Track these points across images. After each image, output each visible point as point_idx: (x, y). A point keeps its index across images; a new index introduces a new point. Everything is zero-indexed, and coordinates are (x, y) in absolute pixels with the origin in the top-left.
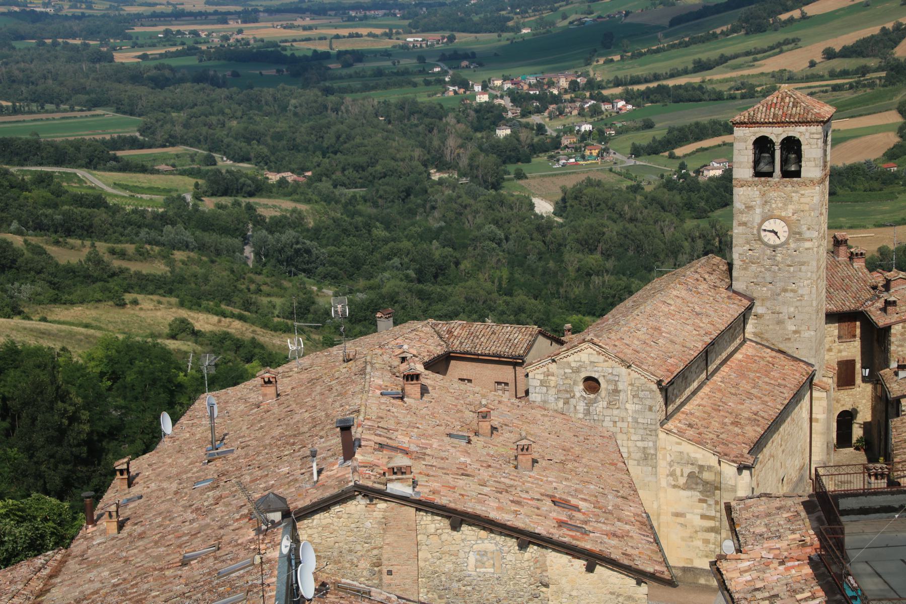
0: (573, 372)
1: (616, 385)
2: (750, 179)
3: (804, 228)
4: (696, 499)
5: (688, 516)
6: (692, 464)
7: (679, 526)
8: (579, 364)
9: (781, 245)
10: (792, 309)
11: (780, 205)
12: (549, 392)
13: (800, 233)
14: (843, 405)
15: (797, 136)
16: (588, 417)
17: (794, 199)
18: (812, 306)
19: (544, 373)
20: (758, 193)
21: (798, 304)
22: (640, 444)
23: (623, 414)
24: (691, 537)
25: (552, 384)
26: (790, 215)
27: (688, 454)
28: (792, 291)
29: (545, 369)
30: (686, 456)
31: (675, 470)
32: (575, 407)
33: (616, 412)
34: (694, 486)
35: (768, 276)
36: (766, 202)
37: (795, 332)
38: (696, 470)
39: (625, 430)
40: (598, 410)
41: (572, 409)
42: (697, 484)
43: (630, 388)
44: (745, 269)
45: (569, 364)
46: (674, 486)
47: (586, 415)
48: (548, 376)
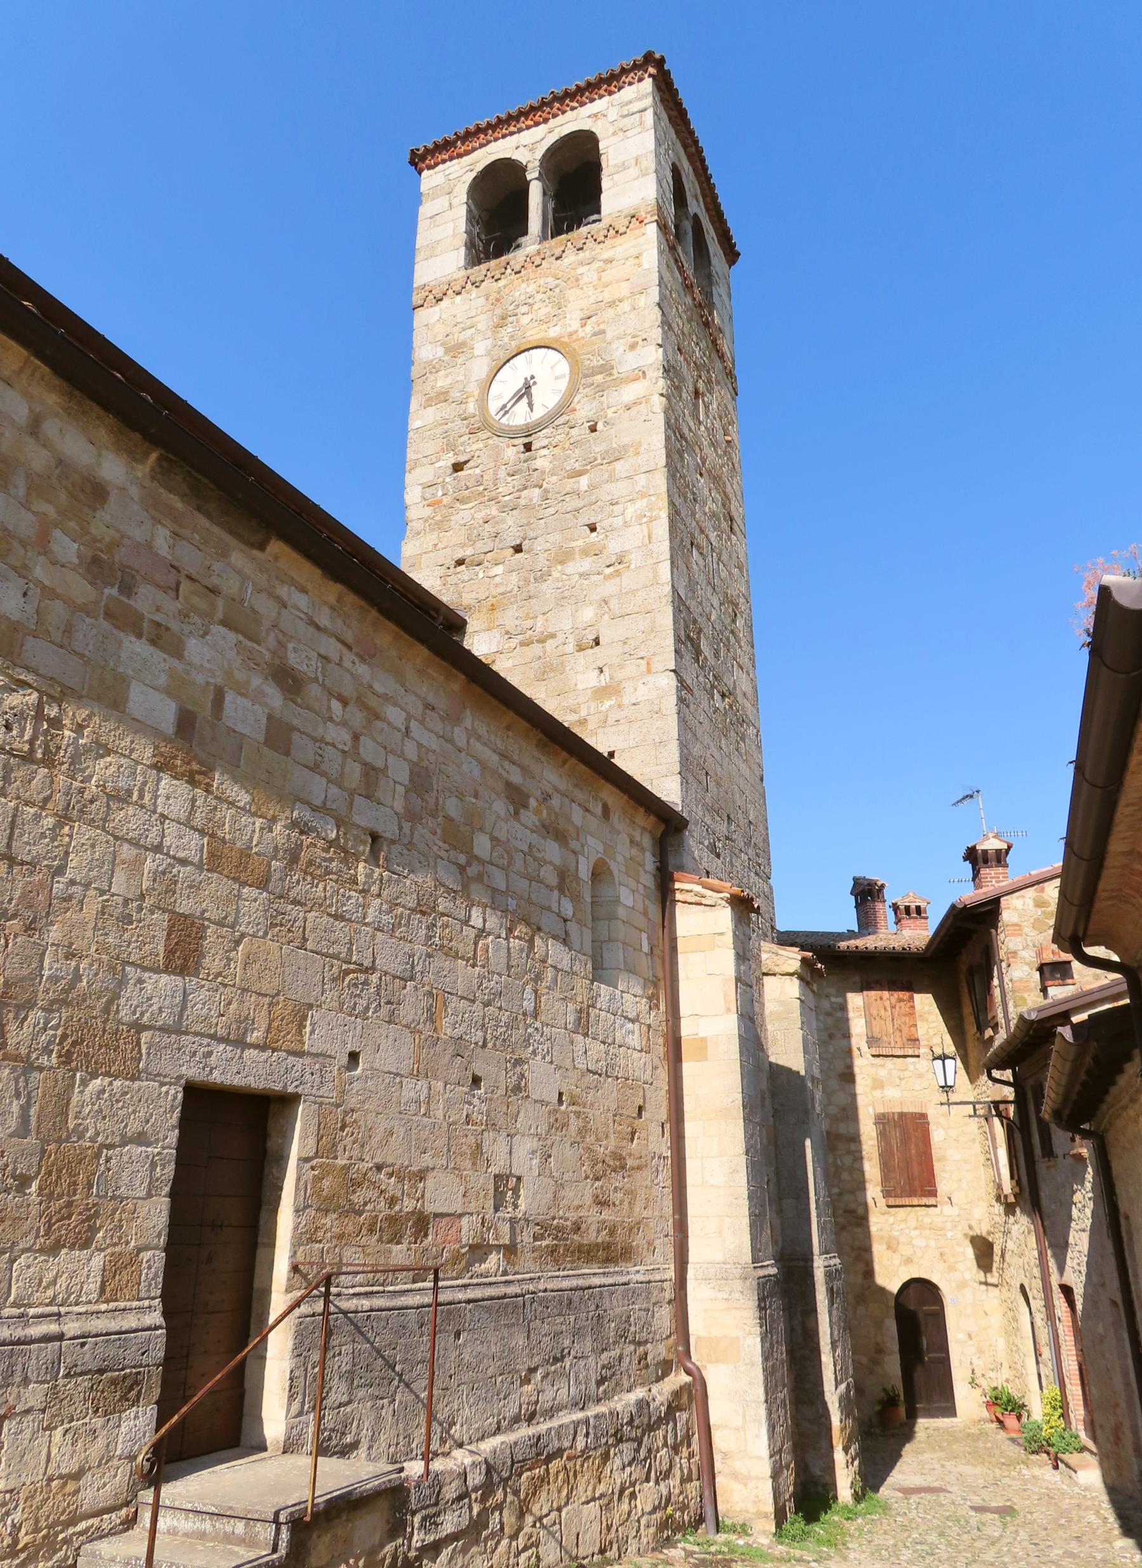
2: (463, 273)
3: (619, 348)
9: (550, 419)
10: (588, 614)
11: (543, 310)
13: (606, 369)
14: (908, 1261)
15: (585, 125)
17: (585, 279)
18: (655, 581)
20: (482, 300)
21: (609, 588)
26: (575, 325)
28: (585, 552)
35: (511, 528)
36: (504, 318)
37: (602, 693)
44: (441, 526)
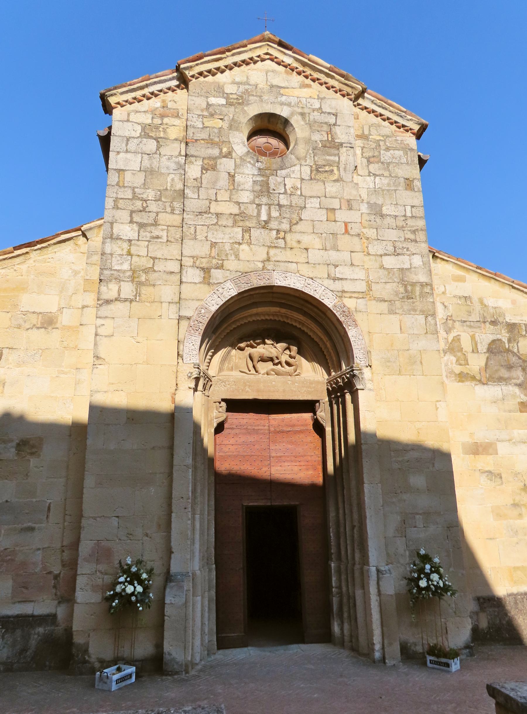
0: (229, 104)
1: (329, 132)
4: (513, 404)
5: (503, 449)
6: (494, 323)
7: (483, 479)
8: (242, 88)
12: (163, 151)
16: (264, 200)
19: (153, 112)
22: (390, 262)
23: (349, 193)
24: (515, 505)
25: (174, 133)
27: (481, 301)
29: (156, 103)
30: (478, 307)
31: (457, 339)
32: (232, 177)
33: (332, 188)
34: (504, 373)
38: (504, 336)
39: (355, 229)
40: (289, 183)
41: (223, 181)
42: (510, 367)
43: (359, 143)
45: (220, 90)
46: (462, 377)
47: (259, 194)
48: (162, 116)
